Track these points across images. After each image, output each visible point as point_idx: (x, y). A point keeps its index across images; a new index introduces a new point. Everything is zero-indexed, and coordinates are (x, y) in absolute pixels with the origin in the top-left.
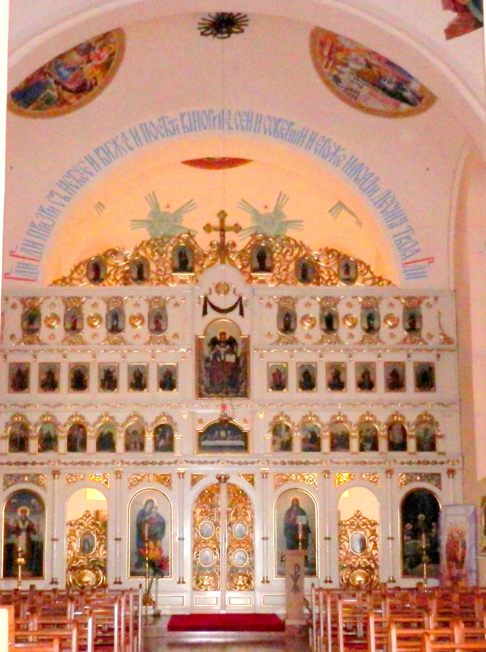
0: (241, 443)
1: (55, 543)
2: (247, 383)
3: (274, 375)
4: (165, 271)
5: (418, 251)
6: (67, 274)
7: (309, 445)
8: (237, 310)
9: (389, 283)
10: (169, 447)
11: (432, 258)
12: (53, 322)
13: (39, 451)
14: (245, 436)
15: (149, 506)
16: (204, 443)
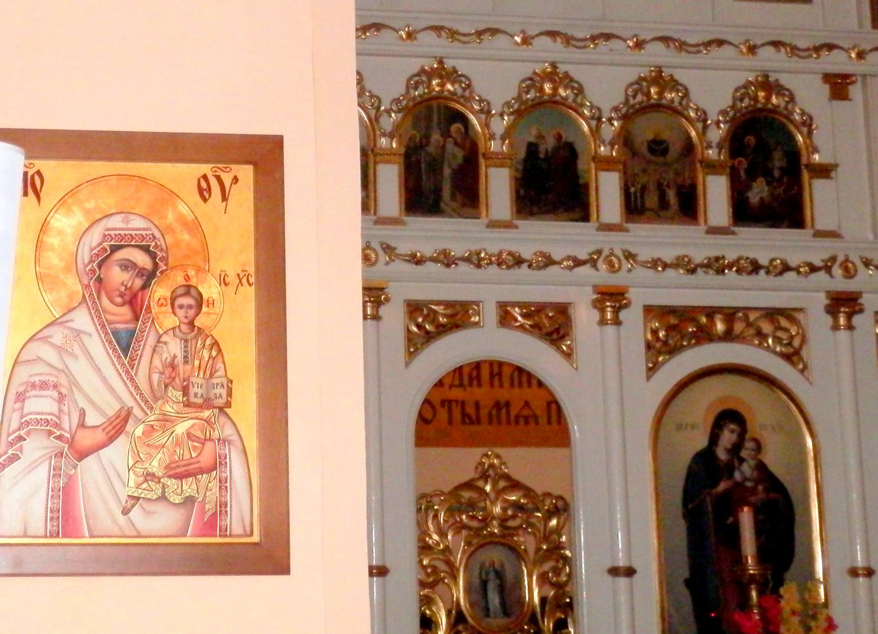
15: (728, 437)
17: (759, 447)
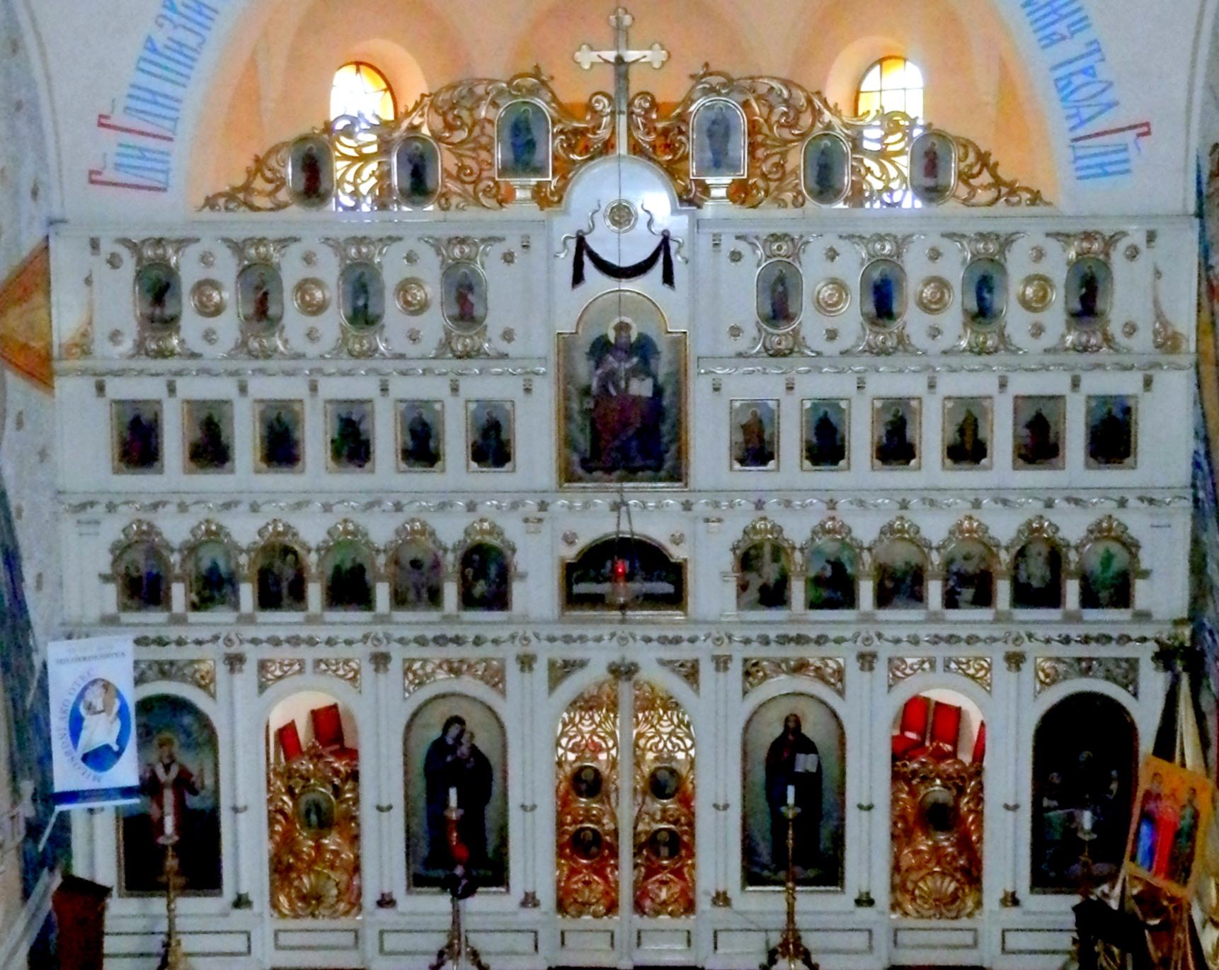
0: (667, 588)
1: (241, 816)
2: (679, 451)
3: (745, 428)
4: (481, 170)
5: (1111, 105)
6: (240, 181)
7: (825, 594)
8: (659, 268)
9: (1036, 198)
10: (498, 600)
11: (1147, 124)
12: (210, 297)
13: (195, 607)
14: (676, 573)
15: (454, 731)
16: (581, 588)
17: (472, 736)
